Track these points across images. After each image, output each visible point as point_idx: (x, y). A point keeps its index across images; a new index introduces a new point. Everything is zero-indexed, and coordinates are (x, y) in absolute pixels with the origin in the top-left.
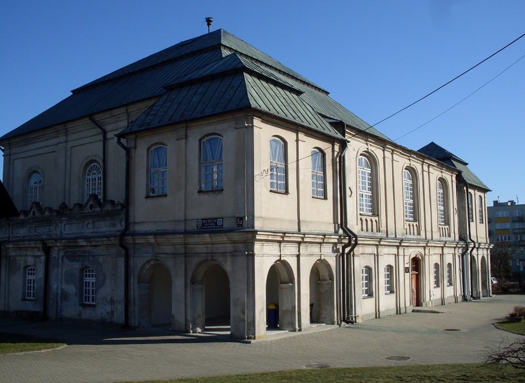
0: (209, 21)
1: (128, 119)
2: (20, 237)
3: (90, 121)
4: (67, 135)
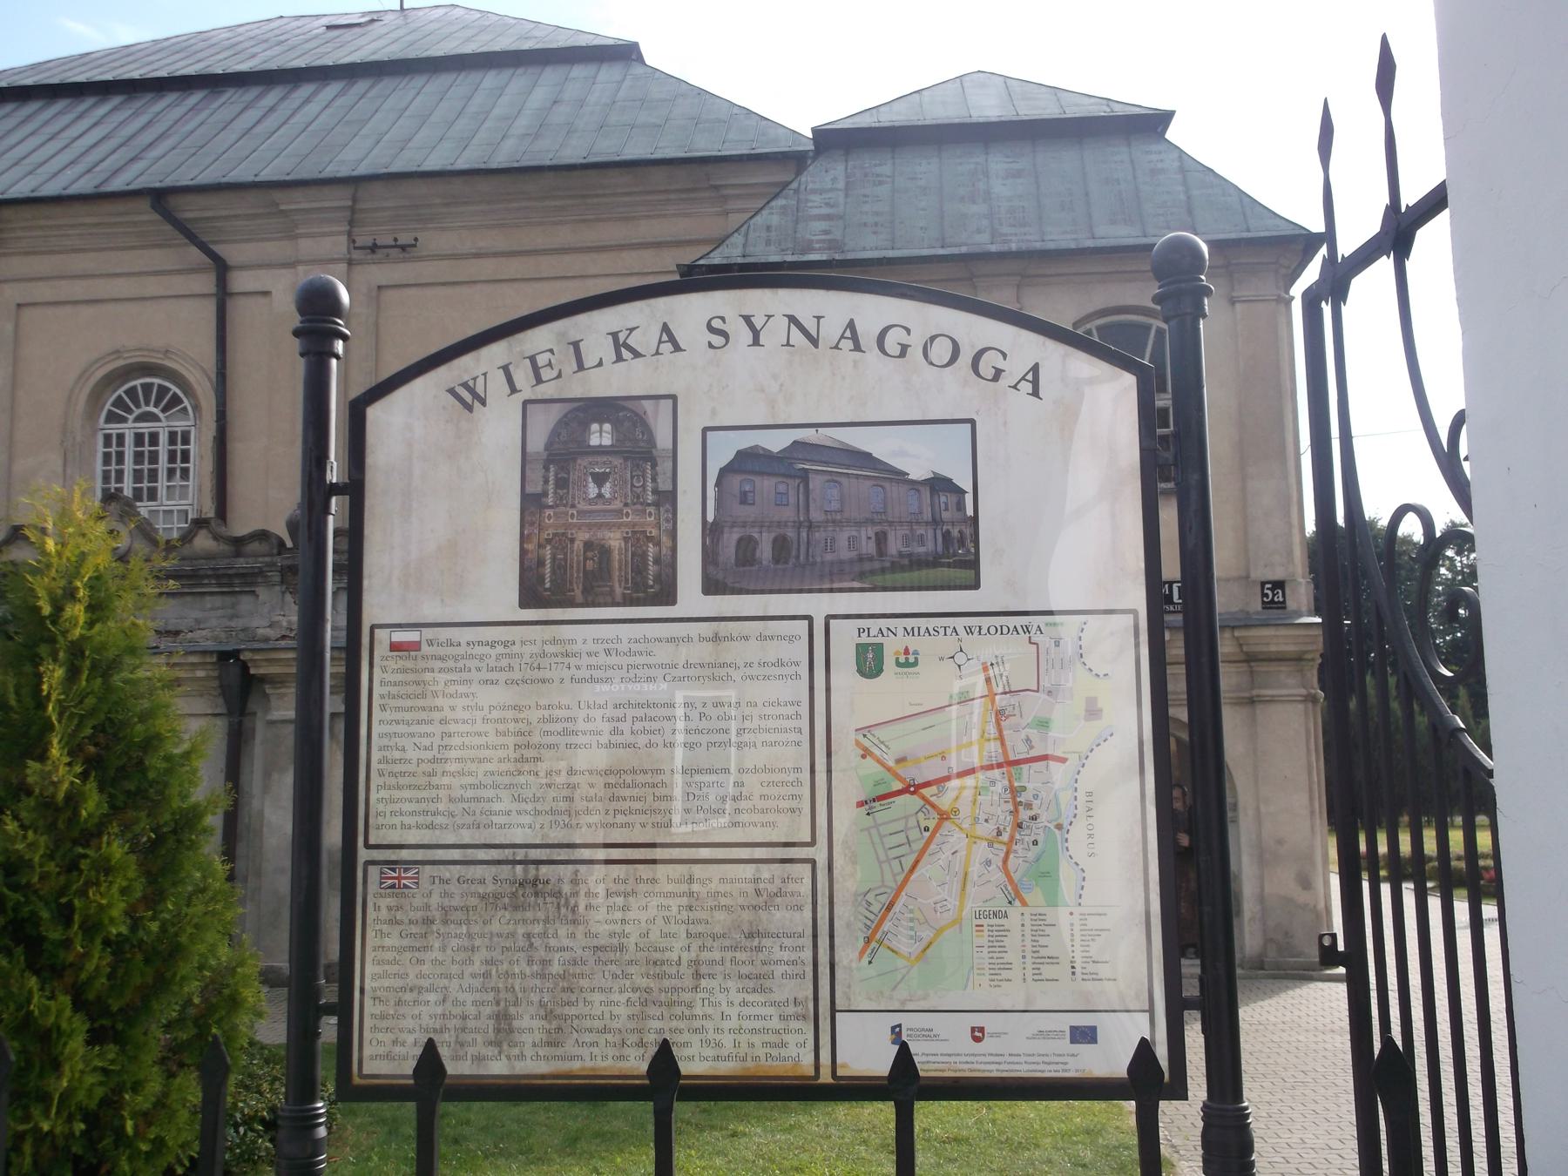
1: (350, 234)
3: (156, 217)
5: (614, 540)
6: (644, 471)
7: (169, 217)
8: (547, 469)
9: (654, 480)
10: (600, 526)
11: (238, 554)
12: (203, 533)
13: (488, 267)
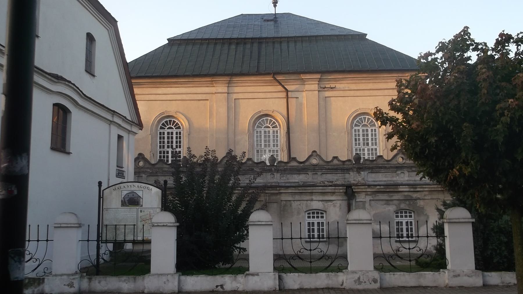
0: (275, 3)
1: (318, 84)
2: (298, 182)
4: (228, 87)
7: (275, 79)
11: (344, 165)
12: (335, 160)
13: (352, 93)
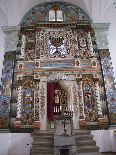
5: (69, 82)
6: (86, 38)
8: (21, 38)
9: (94, 43)
10: (58, 71)
